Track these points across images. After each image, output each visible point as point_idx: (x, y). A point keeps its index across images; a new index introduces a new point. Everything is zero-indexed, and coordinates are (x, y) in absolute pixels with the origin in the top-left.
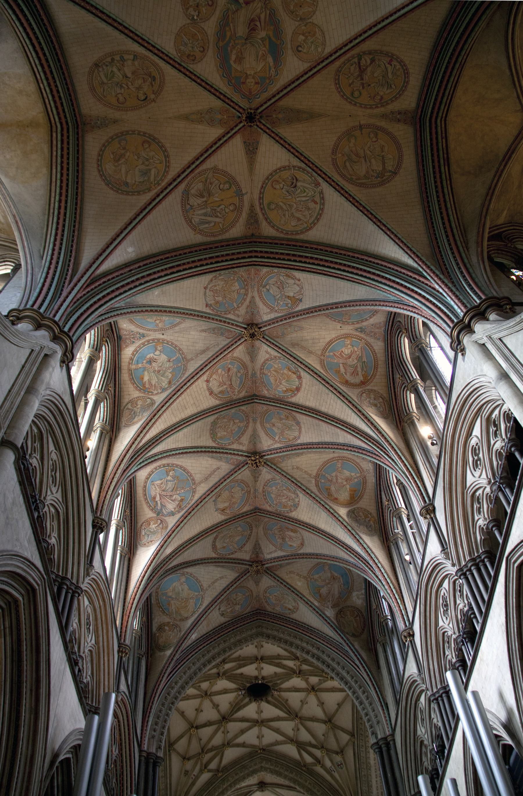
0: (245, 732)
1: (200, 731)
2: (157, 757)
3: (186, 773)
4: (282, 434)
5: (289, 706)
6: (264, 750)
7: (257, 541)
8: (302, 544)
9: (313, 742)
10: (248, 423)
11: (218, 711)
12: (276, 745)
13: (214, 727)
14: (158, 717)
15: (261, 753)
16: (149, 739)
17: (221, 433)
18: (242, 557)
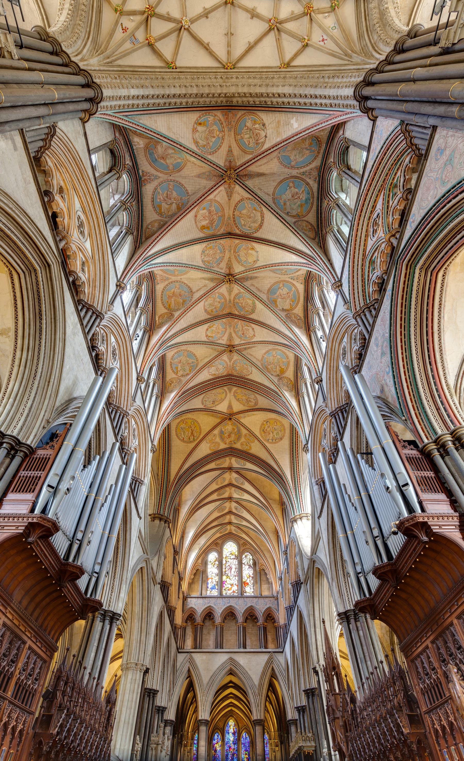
4: (214, 299)
7: (230, 200)
8: (196, 216)
10: (234, 300)
17: (250, 302)
18: (243, 190)
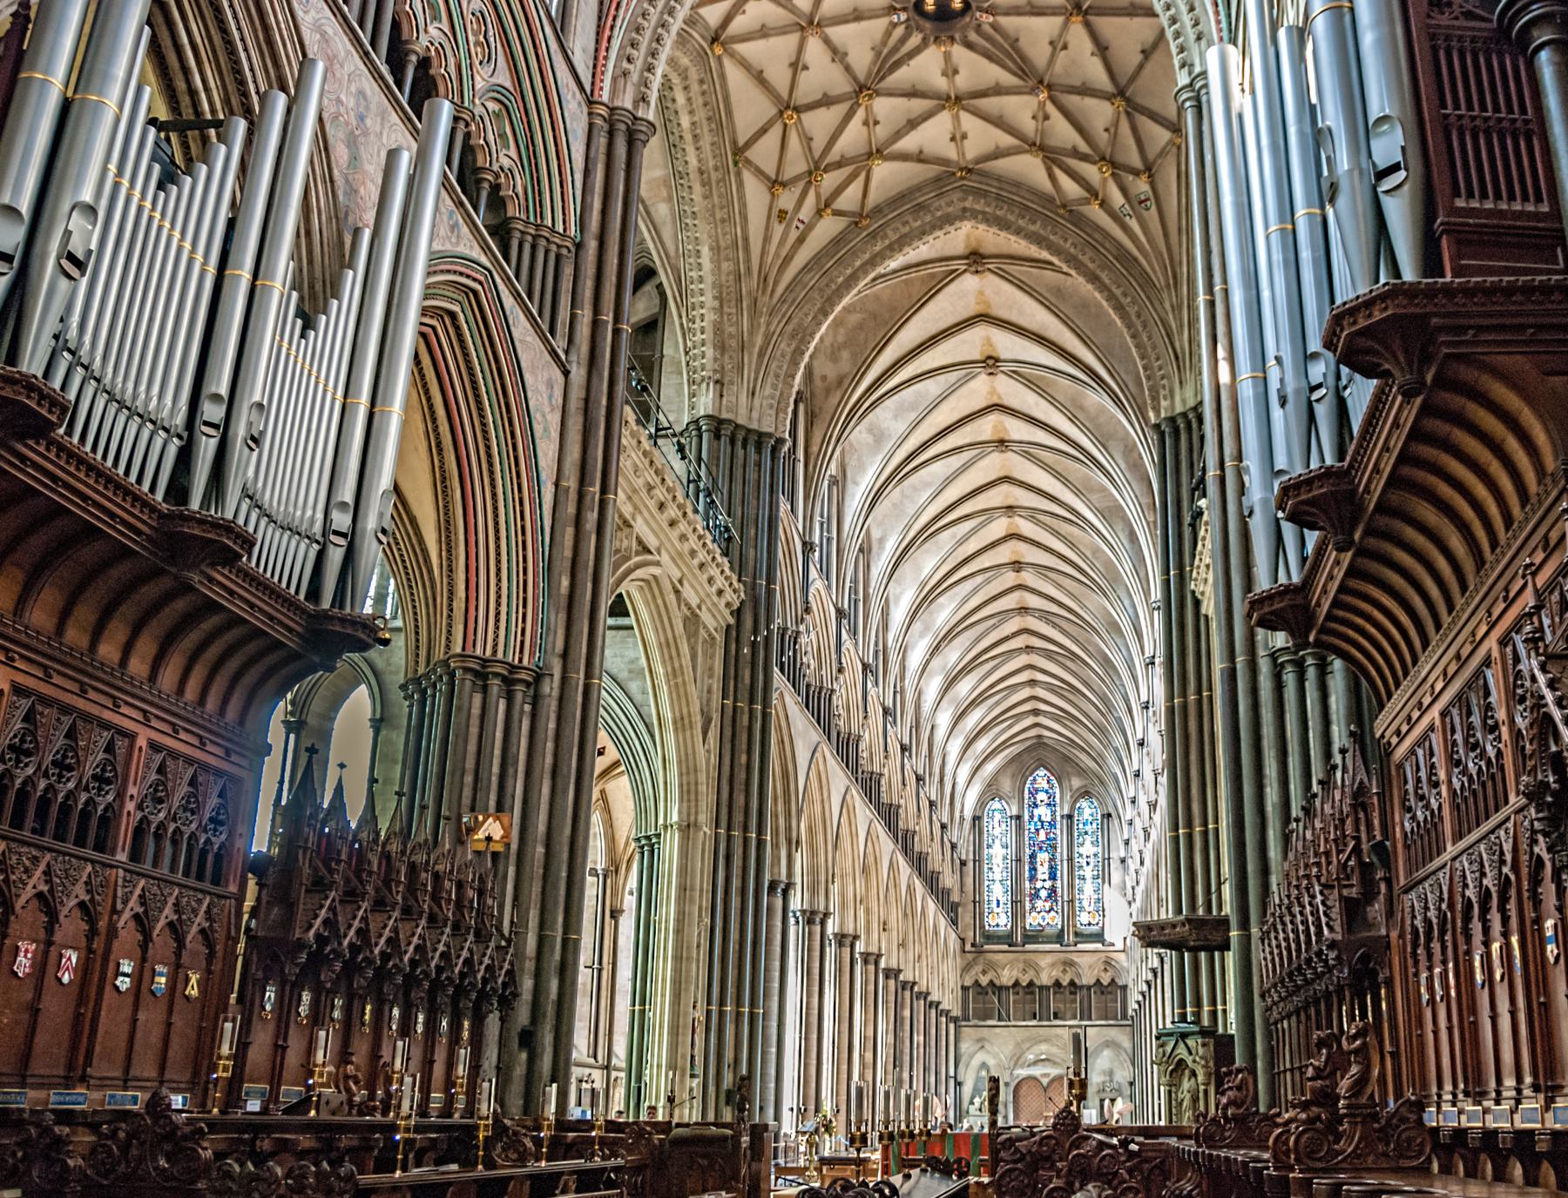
0: (919, 124)
1: (804, 116)
2: (636, 118)
3: (782, 214)
5: (1023, 58)
6: (969, 171)
9: (1083, 147)
11: (848, 68)
12: (996, 158)
13: (840, 110)
14: (638, 30)
15: (962, 178)
16: (614, 79)
